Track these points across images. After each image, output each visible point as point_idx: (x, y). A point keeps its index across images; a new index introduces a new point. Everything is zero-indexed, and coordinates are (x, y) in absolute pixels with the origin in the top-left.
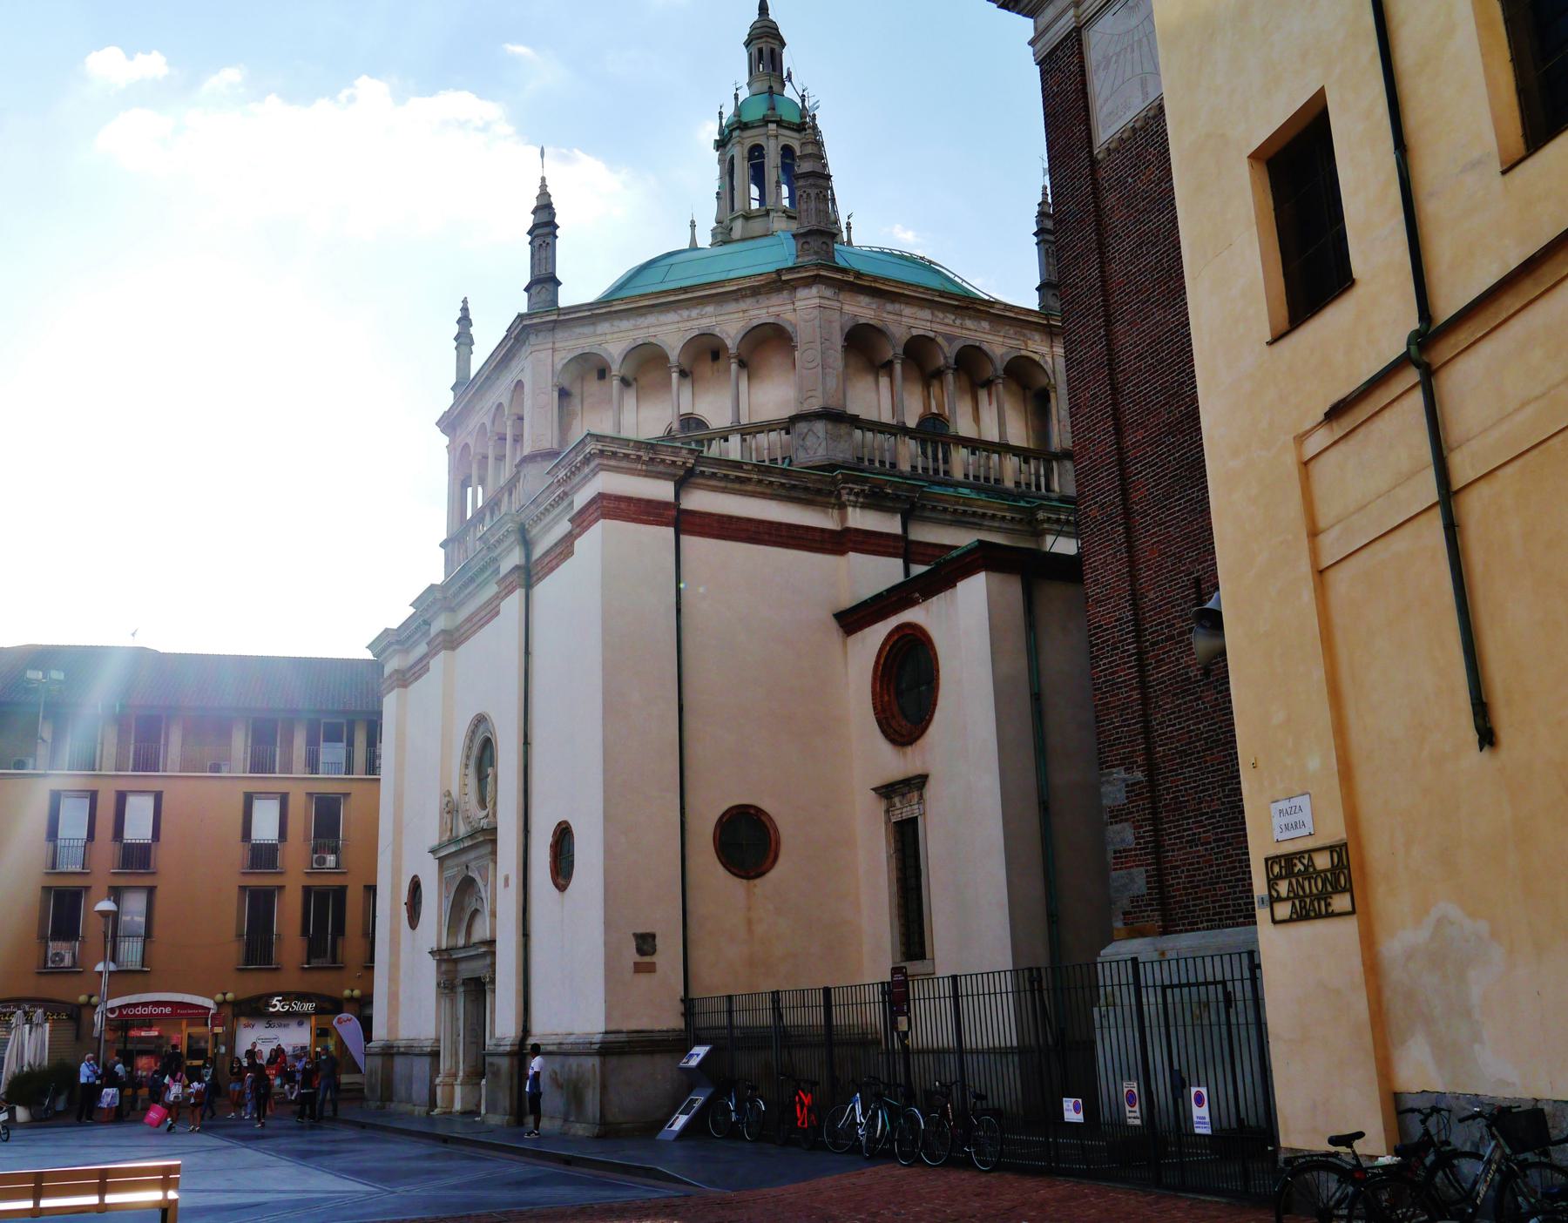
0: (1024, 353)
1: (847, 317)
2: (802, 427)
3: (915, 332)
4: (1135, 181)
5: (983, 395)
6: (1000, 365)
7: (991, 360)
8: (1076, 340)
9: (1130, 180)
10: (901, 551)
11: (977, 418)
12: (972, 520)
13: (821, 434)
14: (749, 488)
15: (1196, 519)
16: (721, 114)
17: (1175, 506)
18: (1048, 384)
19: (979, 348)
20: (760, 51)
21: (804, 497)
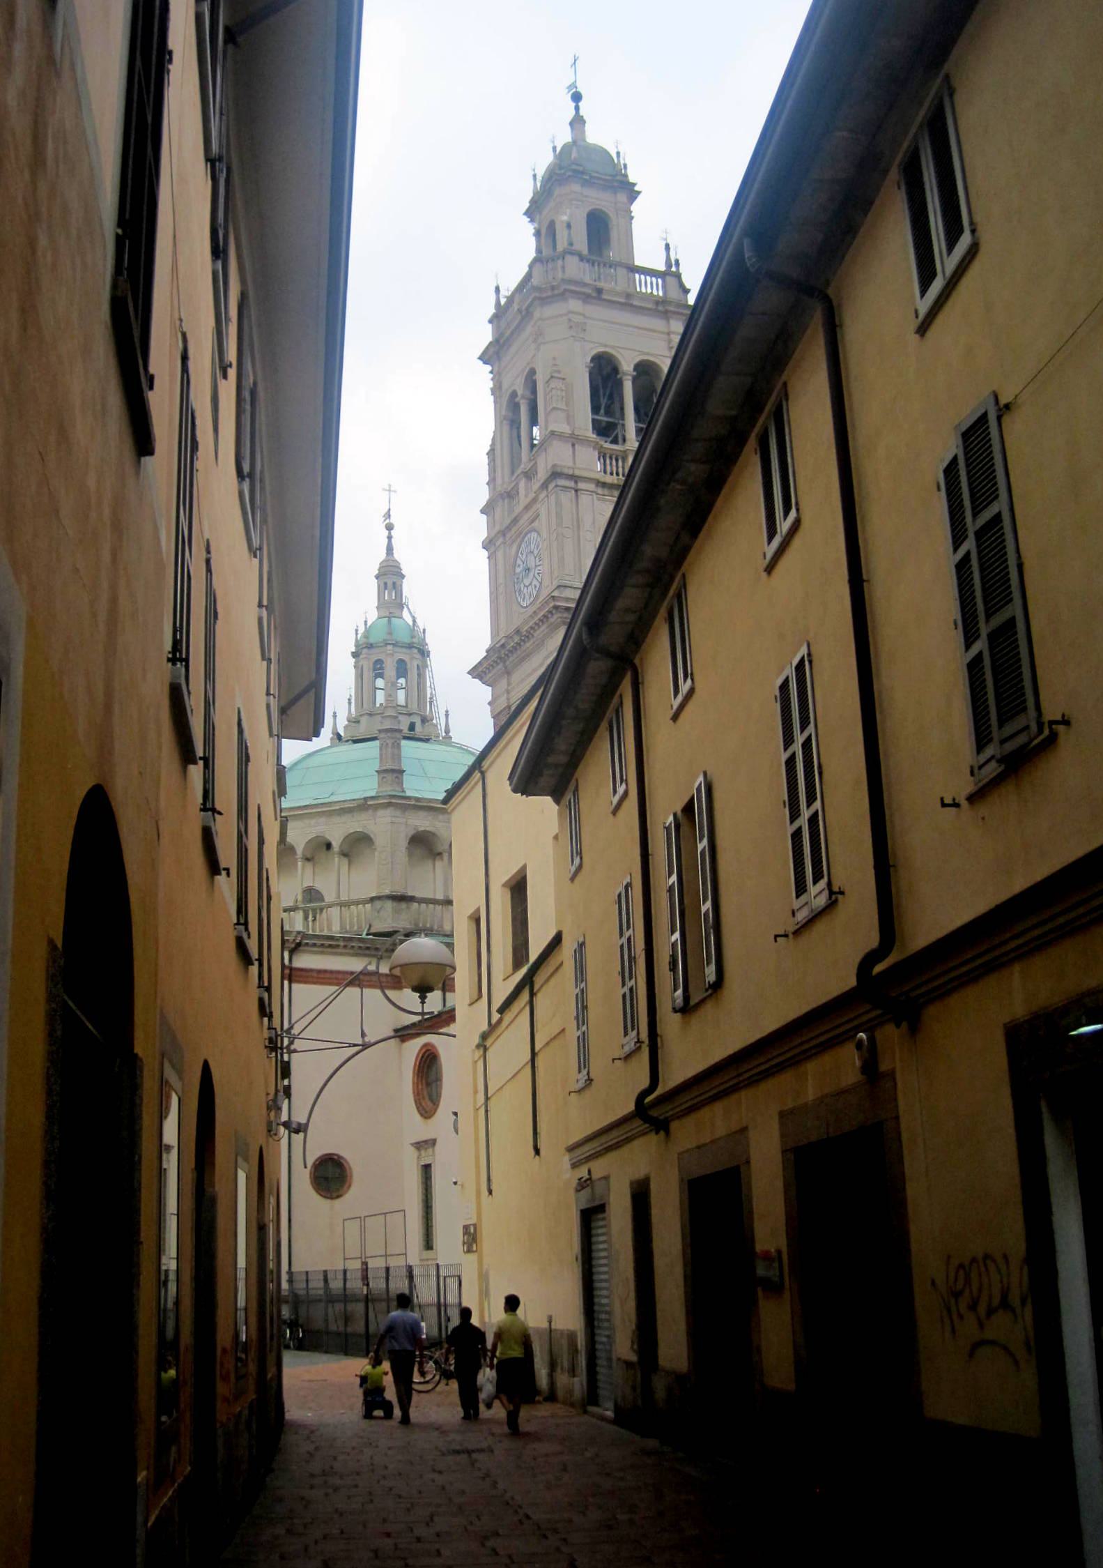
2: (378, 904)
13: (390, 910)
16: (357, 631)
20: (386, 584)
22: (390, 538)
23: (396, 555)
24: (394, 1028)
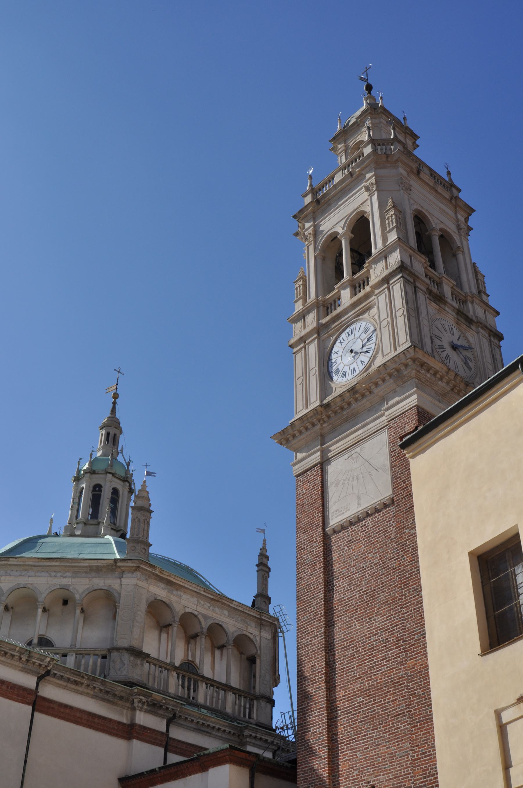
0: (245, 633)
1: (150, 595)
2: (115, 655)
3: (187, 610)
4: (350, 549)
5: (217, 653)
6: (231, 638)
7: (226, 633)
8: (305, 632)
9: (346, 548)
10: (164, 743)
11: (213, 668)
12: (206, 729)
14: (81, 689)
15: (375, 749)
17: (361, 740)
18: (256, 653)
19: (221, 626)
20: (108, 434)
21: (111, 700)
22: (114, 403)
23: (117, 416)
24: (123, 775)
